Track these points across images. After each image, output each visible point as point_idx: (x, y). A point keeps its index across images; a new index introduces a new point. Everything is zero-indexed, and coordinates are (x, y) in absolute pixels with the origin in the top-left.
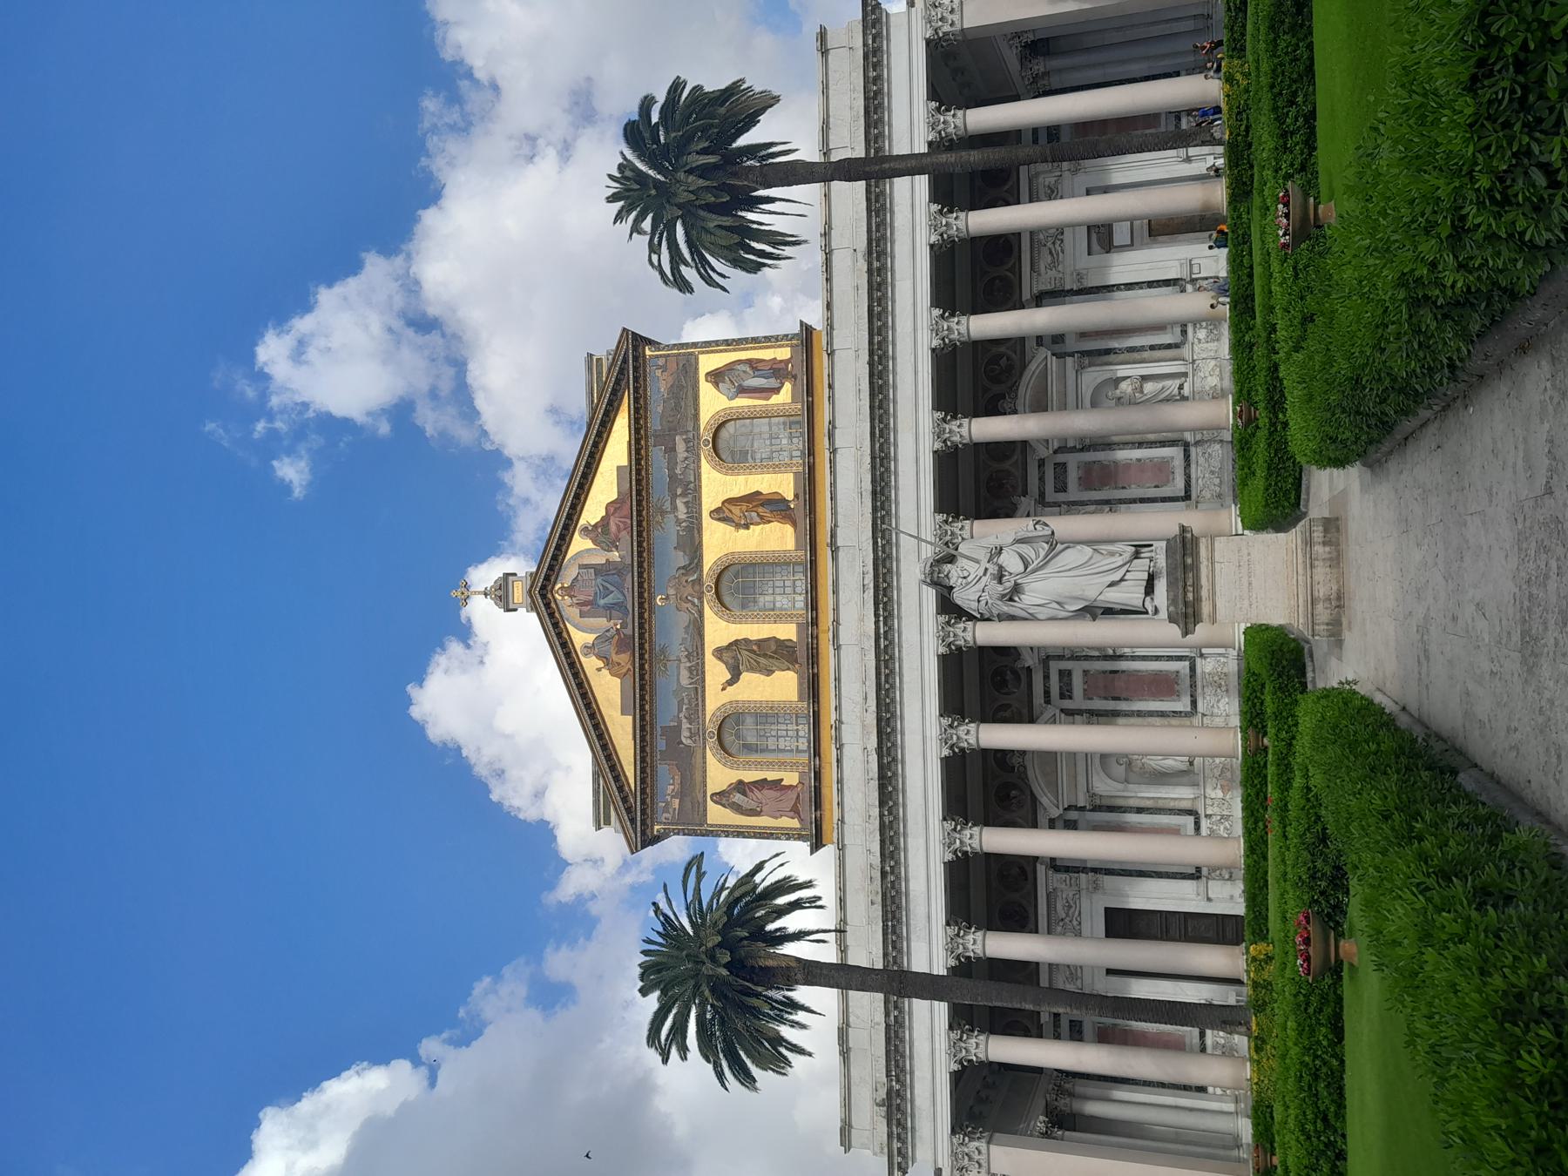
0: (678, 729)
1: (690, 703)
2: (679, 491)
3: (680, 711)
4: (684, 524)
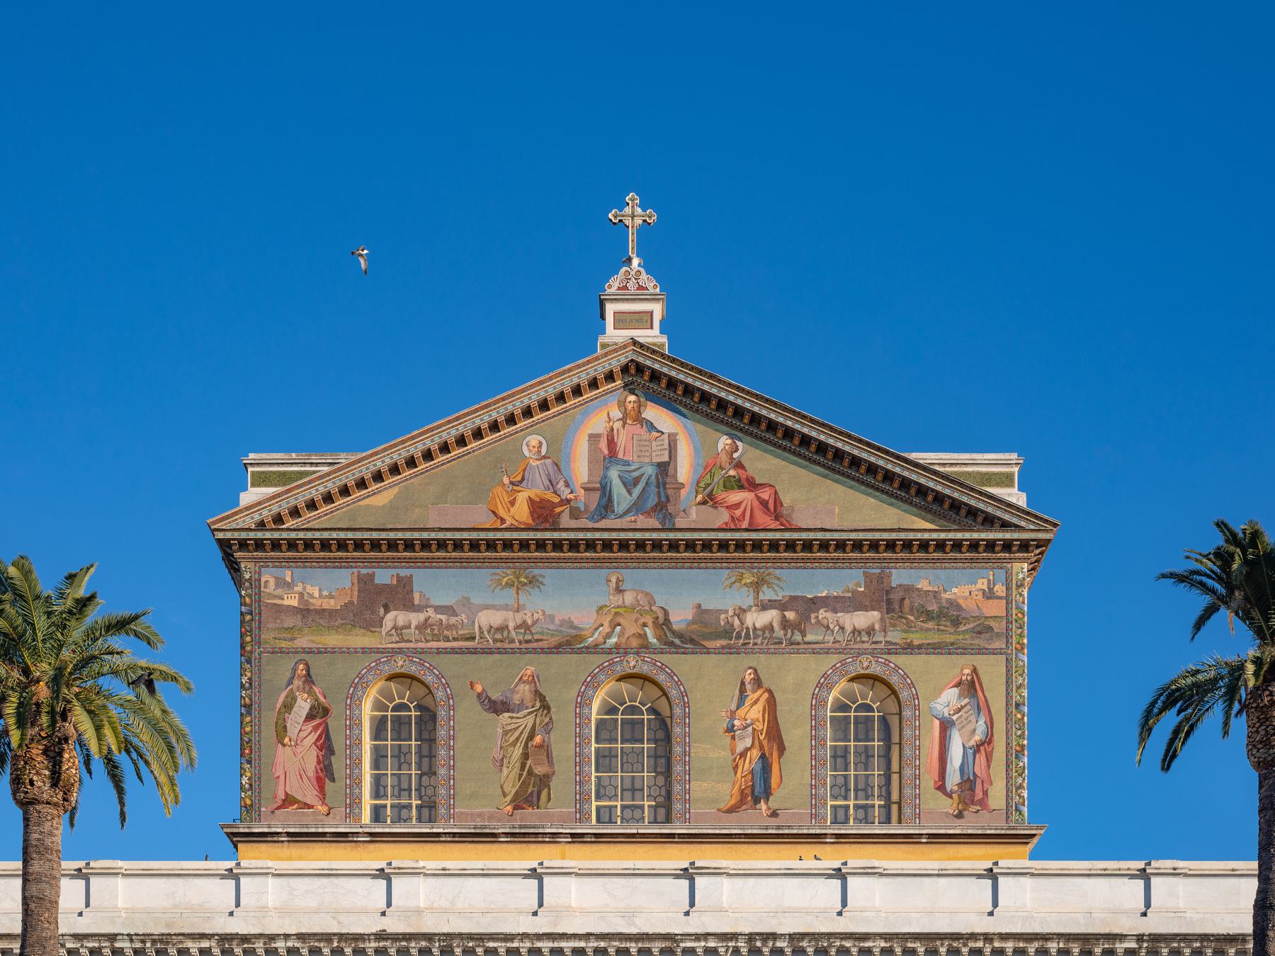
0: (409, 606)
1: (449, 627)
2: (790, 615)
3: (438, 609)
4: (737, 622)
